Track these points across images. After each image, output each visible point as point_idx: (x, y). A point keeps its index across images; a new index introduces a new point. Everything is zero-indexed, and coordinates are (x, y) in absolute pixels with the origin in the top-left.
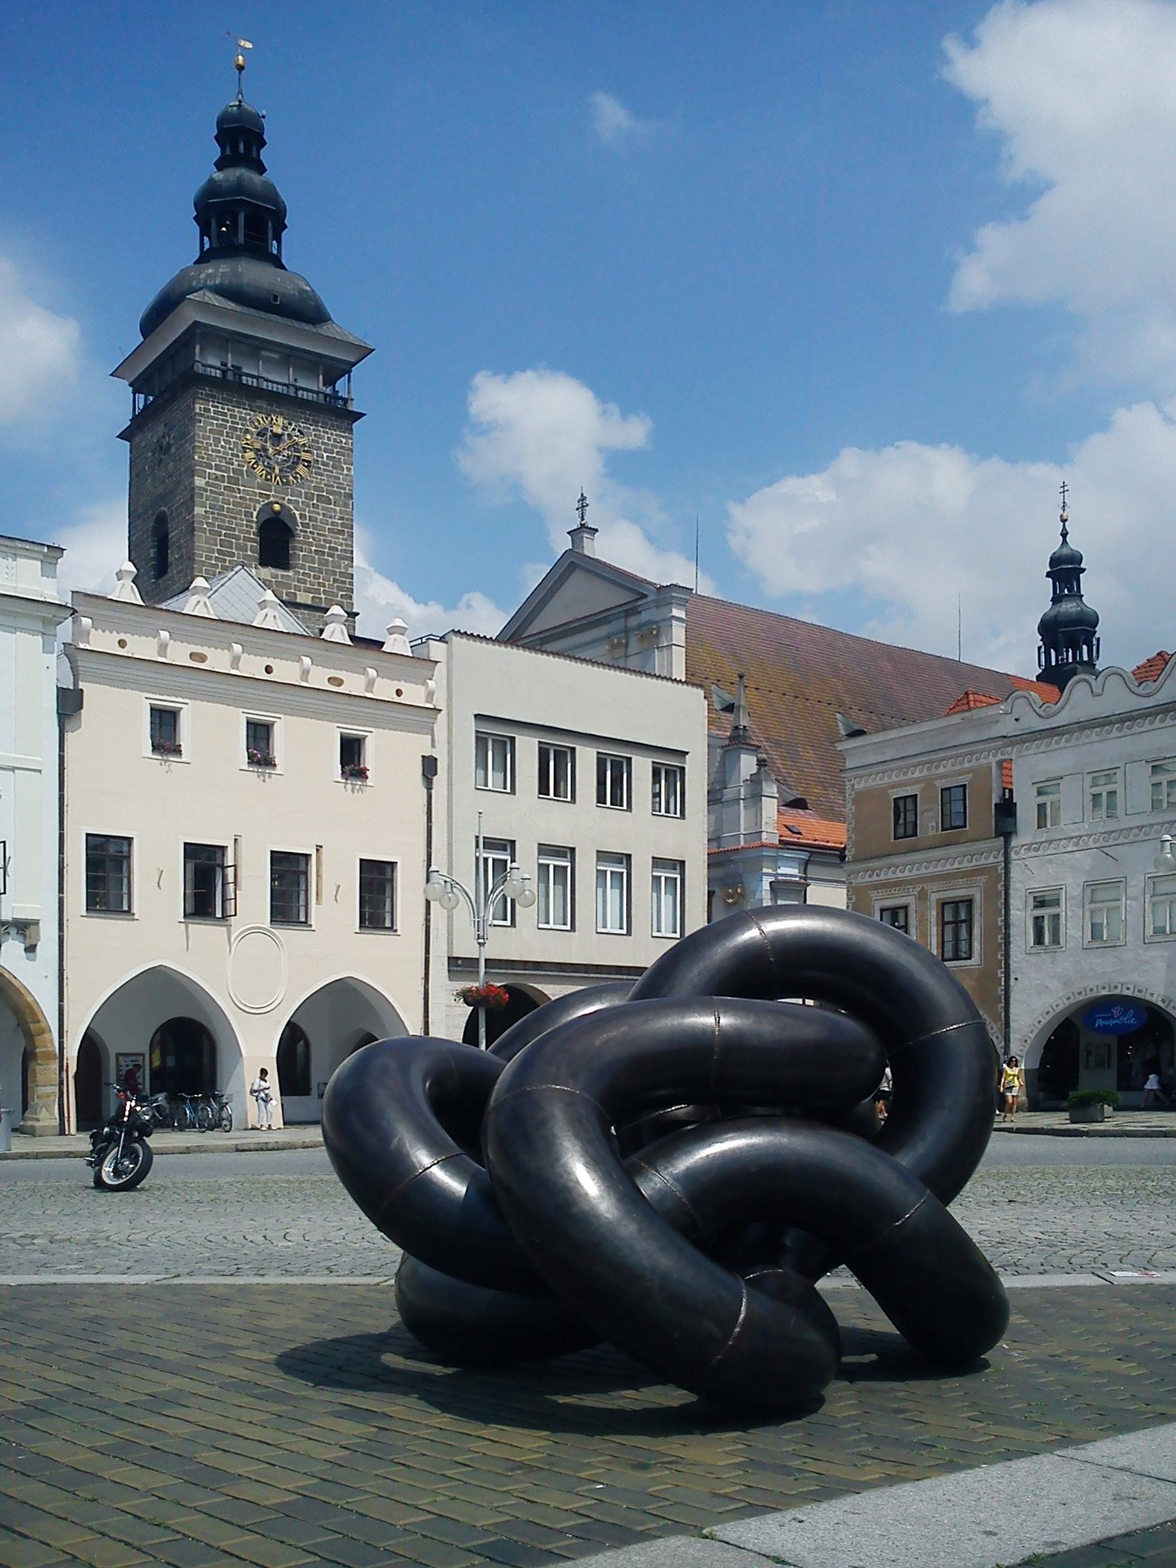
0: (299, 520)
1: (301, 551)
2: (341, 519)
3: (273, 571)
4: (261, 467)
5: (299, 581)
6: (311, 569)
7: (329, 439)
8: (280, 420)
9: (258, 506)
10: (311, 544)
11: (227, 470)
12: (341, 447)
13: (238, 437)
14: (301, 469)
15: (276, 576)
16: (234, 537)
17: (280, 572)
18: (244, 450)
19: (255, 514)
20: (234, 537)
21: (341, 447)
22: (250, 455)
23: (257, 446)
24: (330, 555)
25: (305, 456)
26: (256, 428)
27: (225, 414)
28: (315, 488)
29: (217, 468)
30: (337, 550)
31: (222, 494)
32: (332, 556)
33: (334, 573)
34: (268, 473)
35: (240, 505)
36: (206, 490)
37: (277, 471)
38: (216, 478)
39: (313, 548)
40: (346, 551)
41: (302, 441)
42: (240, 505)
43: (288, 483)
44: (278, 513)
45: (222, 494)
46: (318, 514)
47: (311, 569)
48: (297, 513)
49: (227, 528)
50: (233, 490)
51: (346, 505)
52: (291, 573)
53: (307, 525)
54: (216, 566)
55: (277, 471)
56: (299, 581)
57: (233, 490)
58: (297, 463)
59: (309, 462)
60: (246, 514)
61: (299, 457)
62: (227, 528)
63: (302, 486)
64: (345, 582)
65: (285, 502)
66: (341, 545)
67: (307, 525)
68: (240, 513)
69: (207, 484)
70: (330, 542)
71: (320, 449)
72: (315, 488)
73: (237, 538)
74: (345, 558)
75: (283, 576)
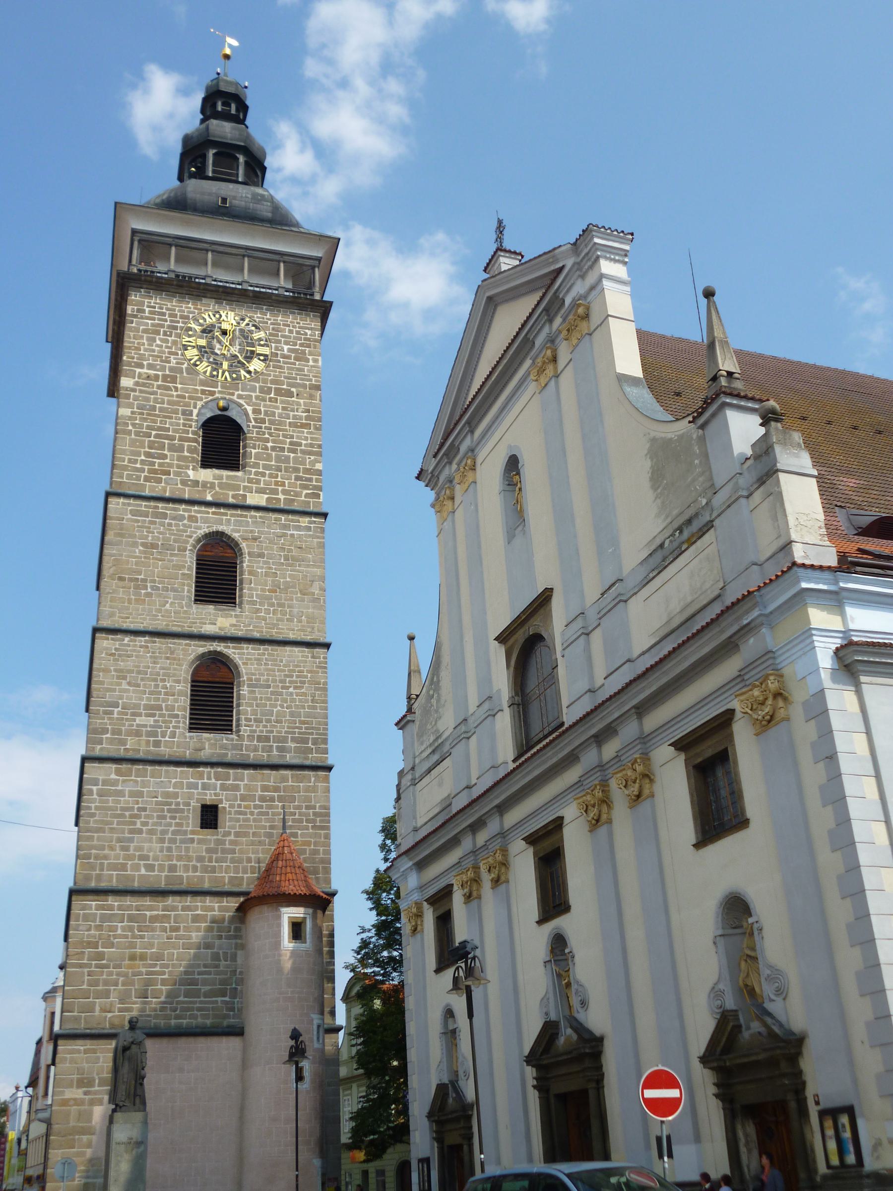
0: (251, 416)
1: (252, 451)
2: (308, 411)
3: (217, 472)
4: (205, 364)
5: (250, 481)
6: (266, 467)
7: (291, 332)
8: (231, 315)
9: (199, 404)
10: (267, 440)
11: (163, 369)
12: (305, 339)
13: (179, 336)
14: (256, 365)
15: (221, 477)
16: (168, 437)
17: (225, 473)
18: (185, 348)
19: (195, 412)
20: (168, 437)
21: (305, 339)
22: (195, 352)
23: (202, 342)
24: (290, 450)
25: (260, 350)
26: (201, 325)
27: (164, 314)
28: (272, 382)
29: (150, 367)
30: (300, 445)
31: (155, 393)
32: (294, 451)
33: (296, 470)
34: (214, 369)
35: (177, 403)
36: (134, 390)
37: (225, 365)
38: (148, 377)
39: (270, 445)
40: (311, 445)
41: (256, 336)
42: (177, 403)
43: (239, 378)
44: (225, 409)
45: (155, 393)
46: (277, 408)
47: (266, 467)
48: (249, 409)
49: (160, 429)
50: (169, 389)
51: (311, 397)
52: (239, 474)
53: (263, 421)
54: (143, 470)
55: (225, 365)
56: (250, 481)
57: (169, 389)
58: (252, 358)
59: (266, 356)
60: (184, 413)
61: (252, 352)
62: (160, 429)
63: (256, 380)
64: (310, 480)
65: (235, 398)
66: (306, 439)
67: (263, 421)
68: (176, 412)
69: (137, 384)
70: (292, 437)
71: (279, 342)
72: (272, 382)
73: (172, 438)
74: (310, 453)
75: (228, 477)
